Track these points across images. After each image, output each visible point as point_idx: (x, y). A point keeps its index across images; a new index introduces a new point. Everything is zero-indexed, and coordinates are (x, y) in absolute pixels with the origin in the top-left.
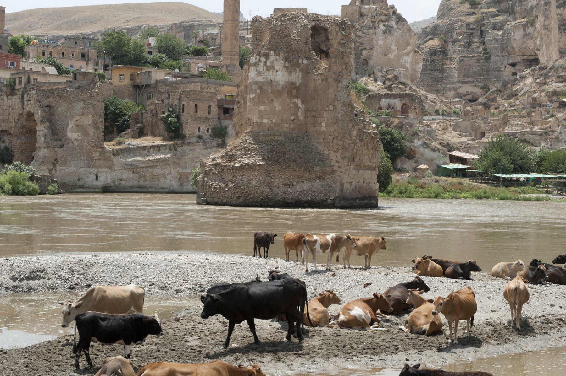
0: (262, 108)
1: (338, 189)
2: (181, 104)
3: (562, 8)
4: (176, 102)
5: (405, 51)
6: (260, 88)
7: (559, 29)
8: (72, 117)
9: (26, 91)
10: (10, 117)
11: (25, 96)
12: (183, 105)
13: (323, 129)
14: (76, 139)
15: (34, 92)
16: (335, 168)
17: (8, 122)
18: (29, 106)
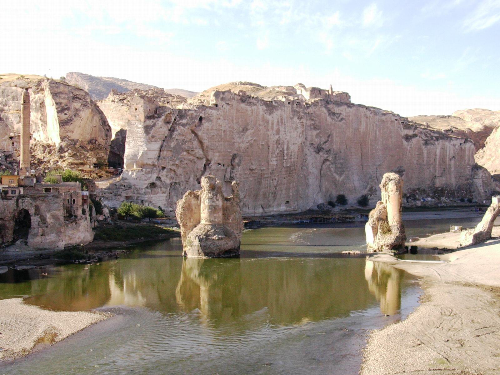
0: (215, 215)
1: (238, 244)
2: (73, 200)
3: (60, 113)
4: (68, 198)
5: (3, 139)
6: (214, 208)
7: (60, 125)
8: (49, 211)
9: (20, 198)
10: (6, 211)
11: (20, 201)
12: (74, 200)
13: (230, 221)
14: (51, 223)
15: (29, 199)
16: (236, 236)
17: (3, 213)
18: (24, 206)
